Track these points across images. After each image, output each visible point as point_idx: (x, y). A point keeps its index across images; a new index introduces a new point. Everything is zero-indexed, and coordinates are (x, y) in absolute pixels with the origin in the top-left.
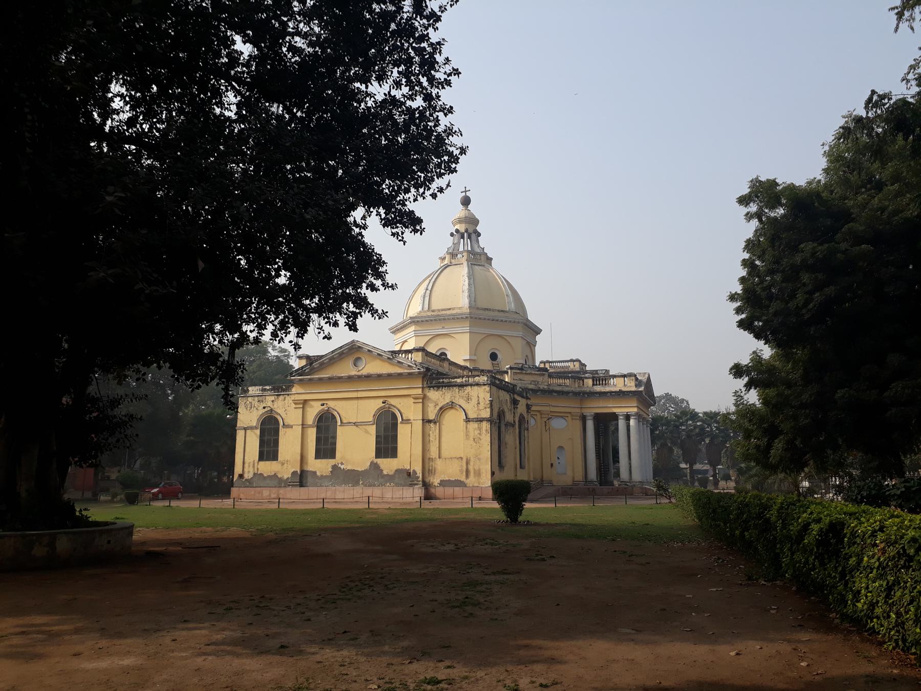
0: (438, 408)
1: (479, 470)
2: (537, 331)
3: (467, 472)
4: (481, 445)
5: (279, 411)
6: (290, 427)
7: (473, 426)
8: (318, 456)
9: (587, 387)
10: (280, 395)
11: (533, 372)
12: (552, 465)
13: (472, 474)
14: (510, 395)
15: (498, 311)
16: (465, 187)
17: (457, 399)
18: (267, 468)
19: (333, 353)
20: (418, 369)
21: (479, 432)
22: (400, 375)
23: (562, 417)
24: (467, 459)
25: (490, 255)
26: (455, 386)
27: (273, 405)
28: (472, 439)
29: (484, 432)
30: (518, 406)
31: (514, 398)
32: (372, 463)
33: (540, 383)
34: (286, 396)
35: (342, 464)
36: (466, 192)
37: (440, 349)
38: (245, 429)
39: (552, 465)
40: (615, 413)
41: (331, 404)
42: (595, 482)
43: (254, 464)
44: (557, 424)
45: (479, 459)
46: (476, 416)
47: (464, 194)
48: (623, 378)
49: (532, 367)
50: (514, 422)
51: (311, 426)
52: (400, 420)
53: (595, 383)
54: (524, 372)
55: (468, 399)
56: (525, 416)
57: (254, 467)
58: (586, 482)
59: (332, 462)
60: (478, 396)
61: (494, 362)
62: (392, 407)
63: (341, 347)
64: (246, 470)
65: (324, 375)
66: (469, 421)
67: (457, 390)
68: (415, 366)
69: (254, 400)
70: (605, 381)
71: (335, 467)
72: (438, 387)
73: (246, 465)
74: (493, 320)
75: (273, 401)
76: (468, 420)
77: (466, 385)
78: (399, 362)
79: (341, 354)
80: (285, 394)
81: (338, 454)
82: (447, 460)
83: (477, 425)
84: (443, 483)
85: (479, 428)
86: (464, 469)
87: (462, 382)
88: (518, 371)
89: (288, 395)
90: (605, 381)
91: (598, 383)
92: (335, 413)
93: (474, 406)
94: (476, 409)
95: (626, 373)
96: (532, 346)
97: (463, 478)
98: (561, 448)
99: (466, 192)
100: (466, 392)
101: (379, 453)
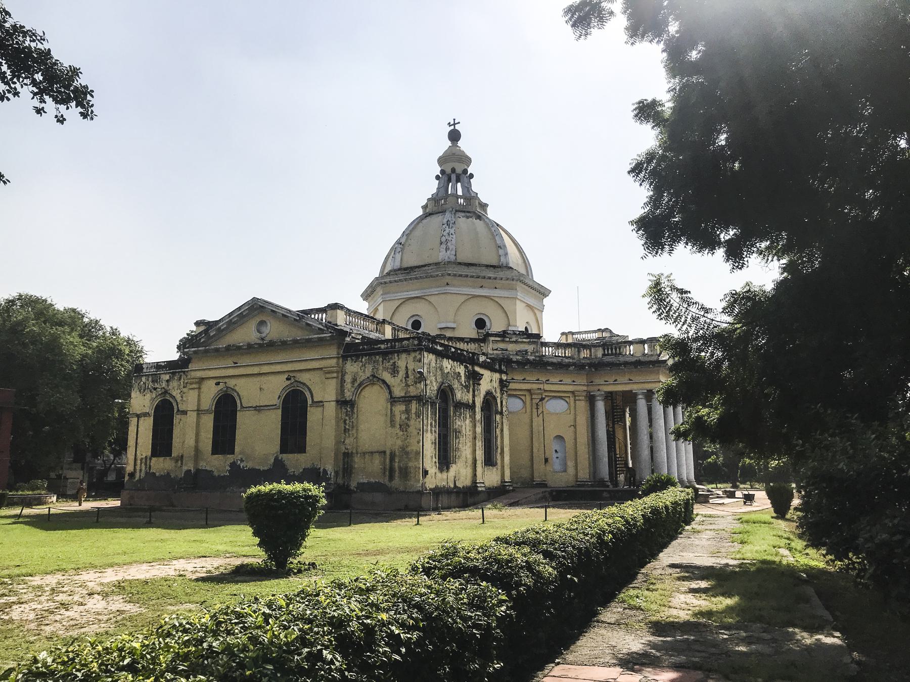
0: (356, 385)
1: (406, 468)
2: (543, 293)
3: (392, 470)
4: (409, 435)
5: (174, 394)
6: (185, 413)
7: (400, 408)
8: (215, 451)
9: (596, 358)
10: (176, 372)
11: (520, 340)
12: (546, 460)
13: (397, 474)
14: (466, 367)
15: (487, 266)
16: (454, 120)
17: (380, 371)
18: (160, 465)
19: (230, 316)
20: (331, 332)
21: (407, 416)
22: (309, 341)
23: (561, 398)
24: (391, 453)
25: (484, 200)
26: (378, 354)
27: (168, 386)
28: (398, 426)
29: (414, 416)
30: (481, 382)
31: (474, 370)
32: (276, 459)
33: (529, 354)
34: (182, 374)
35: (242, 461)
36: (454, 124)
37: (413, 316)
38: (138, 416)
39: (546, 460)
40: (631, 391)
41: (231, 383)
42: (607, 481)
43: (146, 462)
44: (555, 406)
45: (407, 453)
46: (403, 394)
47: (452, 127)
48: (642, 345)
49: (518, 333)
50: (474, 401)
51: (207, 412)
52: (310, 402)
53: (606, 353)
54: (508, 339)
55: (394, 371)
56: (498, 395)
57: (146, 464)
58: (594, 482)
59: (230, 458)
60: (407, 367)
61: (480, 331)
62: (302, 386)
63: (240, 308)
64: (138, 468)
65: (222, 344)
66: (395, 402)
67: (381, 359)
68: (325, 329)
69: (148, 380)
70: (616, 350)
71: (233, 465)
72: (357, 357)
73: (139, 462)
74: (478, 277)
75: (168, 381)
76: (393, 400)
77: (392, 353)
78: (308, 325)
79: (241, 316)
80: (181, 372)
81: (237, 449)
82: (367, 456)
83: (404, 407)
84: (362, 487)
85: (406, 410)
86: (388, 467)
87: (387, 348)
88: (499, 339)
89: (184, 372)
90: (616, 350)
91: (610, 352)
92: (235, 395)
93: (401, 381)
94: (404, 385)
95: (645, 338)
96: (536, 311)
97: (385, 481)
98: (559, 438)
99: (454, 124)
100: (392, 361)
101: (284, 449)
